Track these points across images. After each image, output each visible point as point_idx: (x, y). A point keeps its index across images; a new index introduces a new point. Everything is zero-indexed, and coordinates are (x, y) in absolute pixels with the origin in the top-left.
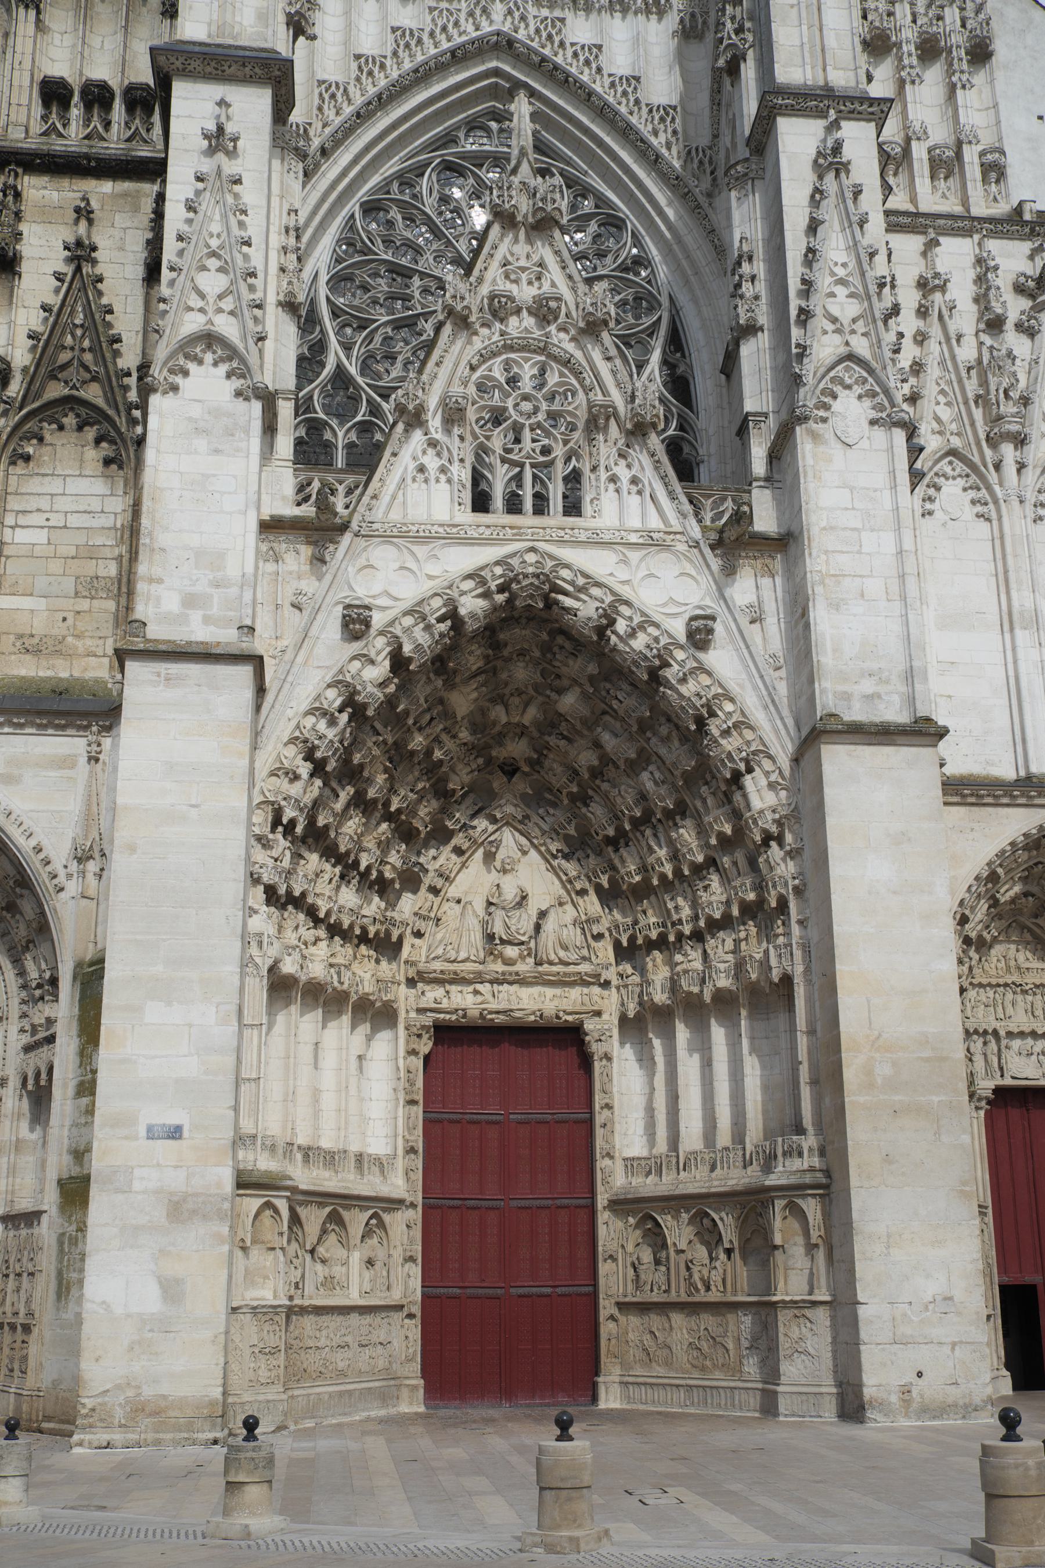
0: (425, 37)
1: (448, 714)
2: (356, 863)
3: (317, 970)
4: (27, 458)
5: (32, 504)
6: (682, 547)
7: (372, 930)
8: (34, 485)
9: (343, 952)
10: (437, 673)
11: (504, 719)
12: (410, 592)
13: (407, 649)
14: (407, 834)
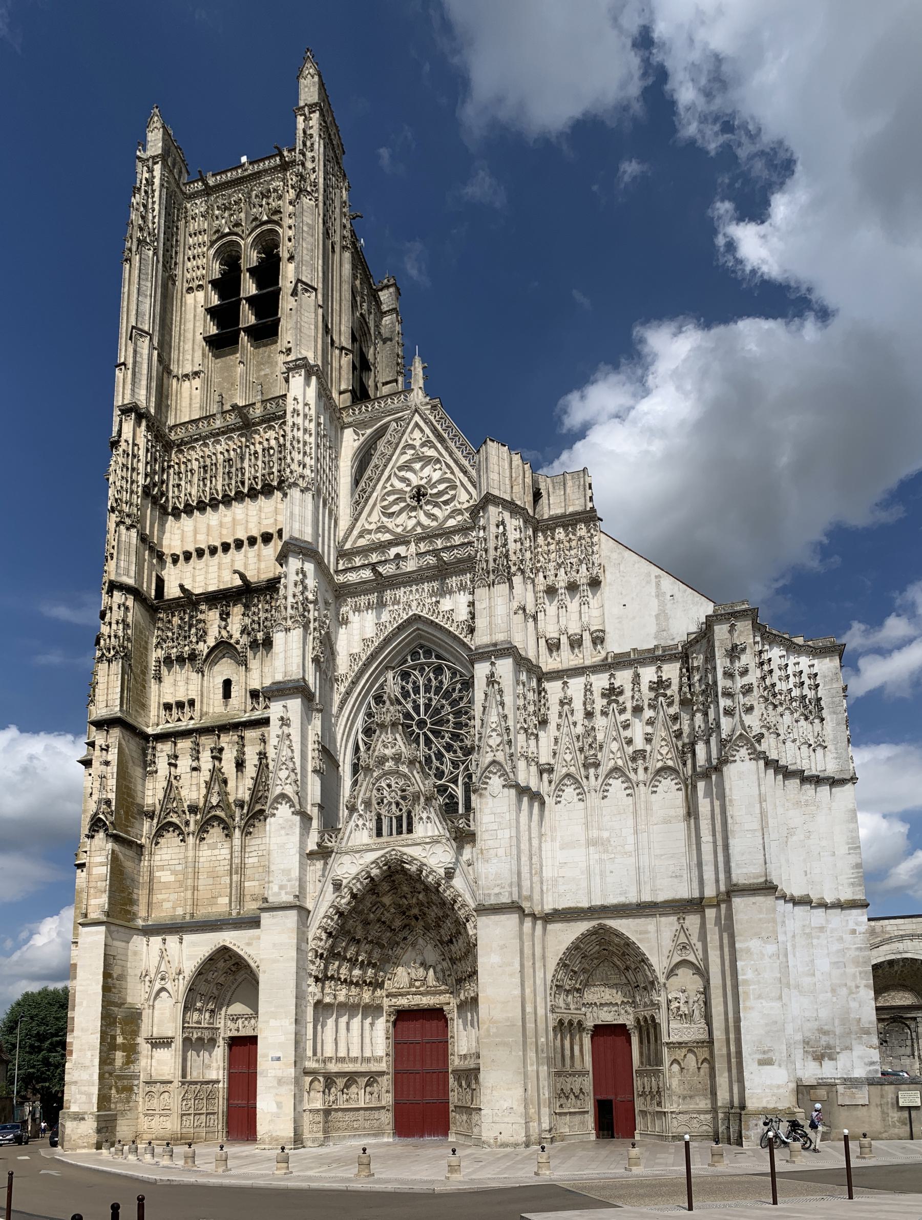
0: (387, 624)
1: (384, 906)
2: (357, 960)
3: (341, 998)
4: (251, 833)
5: (253, 848)
6: (444, 841)
7: (368, 981)
8: (254, 842)
9: (354, 991)
10: (374, 894)
11: (407, 903)
12: (354, 870)
13: (355, 891)
14: (382, 947)
